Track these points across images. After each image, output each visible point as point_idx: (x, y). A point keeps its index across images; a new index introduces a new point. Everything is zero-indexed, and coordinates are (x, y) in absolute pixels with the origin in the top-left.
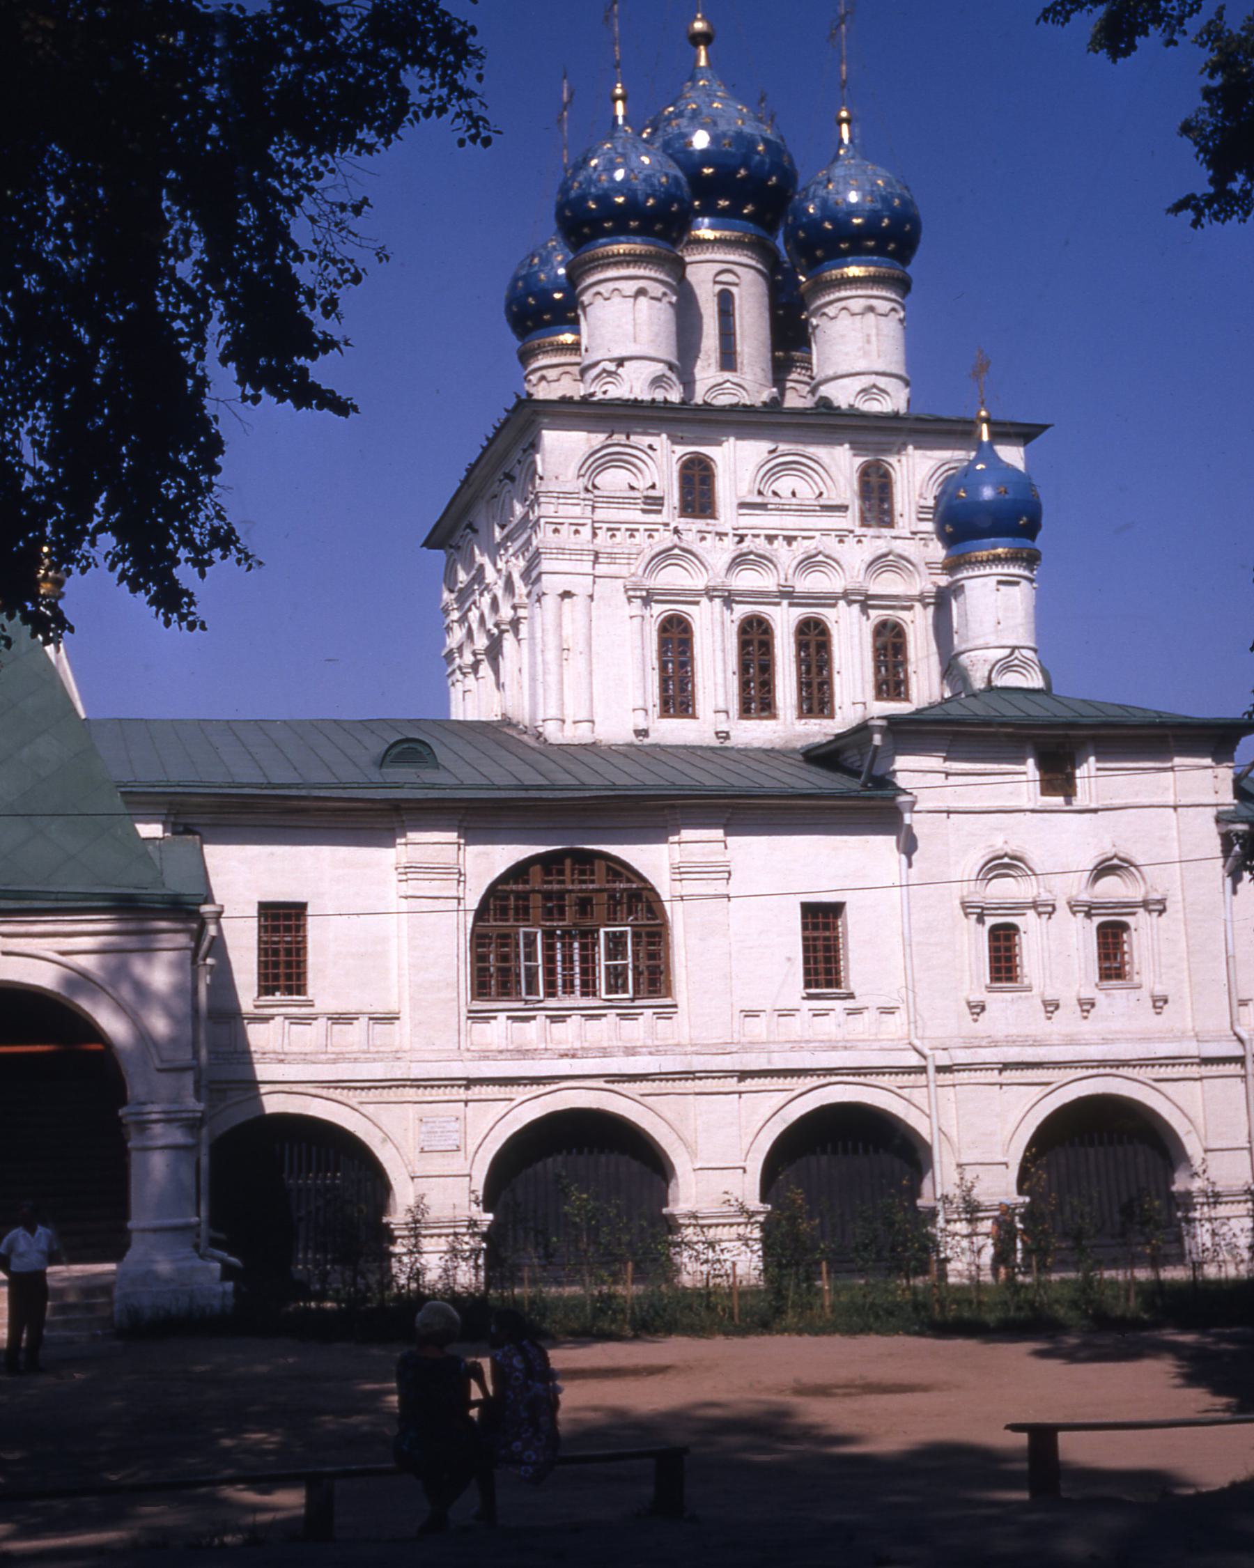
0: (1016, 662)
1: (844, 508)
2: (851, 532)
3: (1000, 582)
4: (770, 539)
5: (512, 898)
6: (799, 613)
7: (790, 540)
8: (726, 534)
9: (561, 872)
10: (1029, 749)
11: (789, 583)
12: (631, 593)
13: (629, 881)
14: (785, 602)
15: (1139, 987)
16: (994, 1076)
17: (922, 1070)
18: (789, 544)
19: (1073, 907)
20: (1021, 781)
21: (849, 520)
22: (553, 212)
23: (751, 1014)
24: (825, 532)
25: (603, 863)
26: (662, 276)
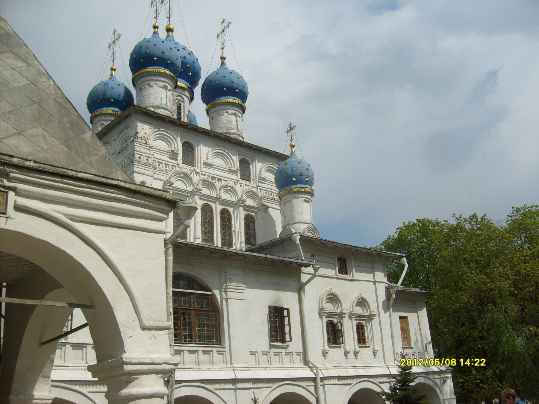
2: (239, 181)
3: (305, 201)
4: (213, 178)
8: (199, 173)
14: (218, 203)
15: (369, 347)
16: (336, 381)
17: (314, 380)
21: (237, 177)
23: (252, 353)
26: (171, 84)
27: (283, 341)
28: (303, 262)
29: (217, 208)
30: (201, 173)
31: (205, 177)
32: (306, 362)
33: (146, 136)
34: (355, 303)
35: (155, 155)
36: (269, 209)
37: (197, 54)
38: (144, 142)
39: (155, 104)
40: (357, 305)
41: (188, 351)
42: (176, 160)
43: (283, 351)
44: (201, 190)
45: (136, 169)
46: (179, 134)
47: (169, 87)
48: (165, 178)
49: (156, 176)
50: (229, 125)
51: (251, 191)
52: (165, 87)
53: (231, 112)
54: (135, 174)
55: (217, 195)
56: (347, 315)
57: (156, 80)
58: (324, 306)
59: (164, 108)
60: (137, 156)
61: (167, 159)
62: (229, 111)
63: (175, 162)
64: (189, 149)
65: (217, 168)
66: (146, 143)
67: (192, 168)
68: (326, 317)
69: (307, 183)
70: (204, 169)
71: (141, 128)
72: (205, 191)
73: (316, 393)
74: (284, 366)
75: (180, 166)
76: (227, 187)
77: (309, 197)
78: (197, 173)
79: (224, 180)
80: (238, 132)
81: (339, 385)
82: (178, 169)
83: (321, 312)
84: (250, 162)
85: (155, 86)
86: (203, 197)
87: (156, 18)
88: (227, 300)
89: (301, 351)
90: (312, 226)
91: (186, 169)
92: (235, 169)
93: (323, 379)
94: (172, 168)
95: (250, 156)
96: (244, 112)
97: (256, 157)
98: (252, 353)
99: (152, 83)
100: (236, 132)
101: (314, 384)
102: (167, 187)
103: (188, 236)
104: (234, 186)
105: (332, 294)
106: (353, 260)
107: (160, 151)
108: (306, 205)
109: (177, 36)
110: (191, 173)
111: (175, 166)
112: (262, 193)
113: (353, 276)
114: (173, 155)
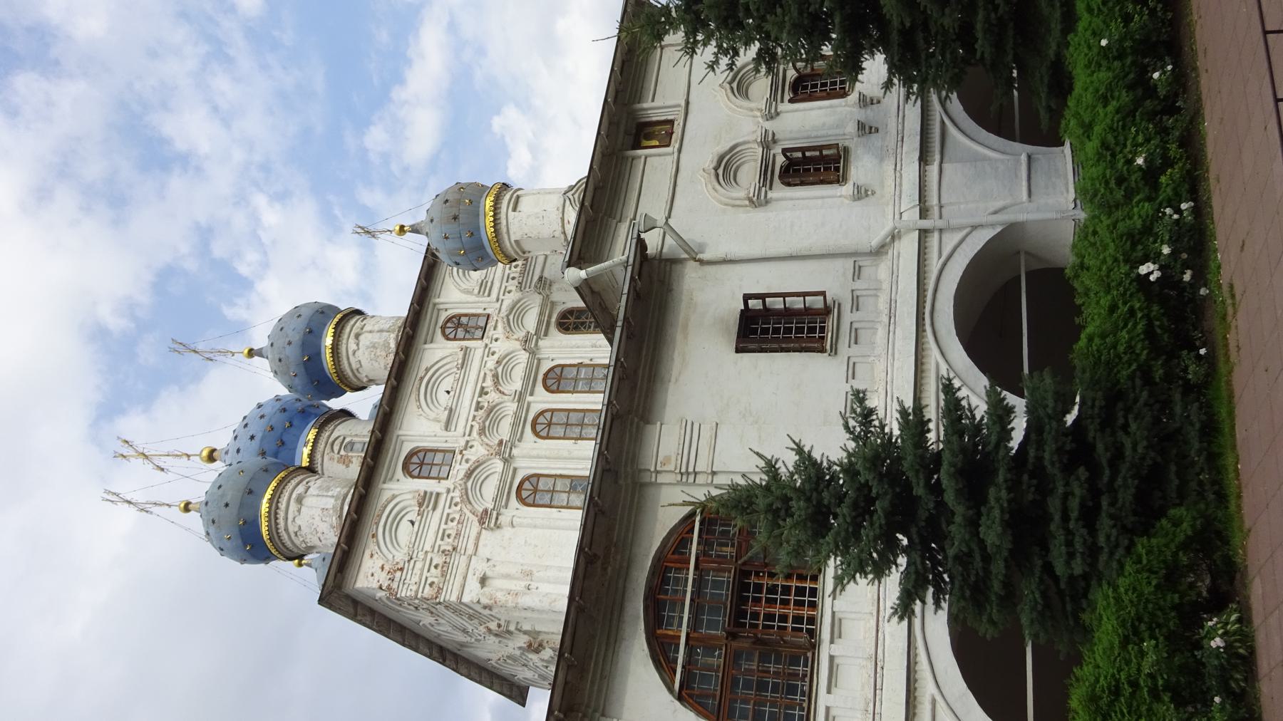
3: (514, 210)
6: (539, 388)
7: (483, 392)
8: (468, 442)
12: (492, 525)
14: (529, 398)
16: (933, 170)
17: (924, 234)
18: (486, 393)
19: (772, 115)
20: (654, 167)
22: (262, 565)
24: (483, 363)
27: (827, 311)
28: (631, 260)
29: (542, 400)
30: (467, 438)
31: (476, 427)
32: (879, 251)
33: (387, 568)
34: (741, 102)
35: (428, 547)
36: (546, 275)
37: (248, 408)
38: (399, 573)
40: (746, 96)
42: (438, 494)
43: (847, 317)
44: (501, 442)
45: (454, 598)
46: (385, 486)
47: (301, 489)
48: (475, 527)
49: (470, 550)
51: (508, 316)
52: (300, 500)
53: (352, 346)
54: (466, 599)
56: (769, 125)
57: (286, 519)
58: (742, 194)
60: (428, 592)
64: (419, 463)
66: (402, 569)
68: (771, 188)
69: (475, 204)
70: (460, 429)
71: (370, 578)
72: (505, 430)
73: (960, 228)
76: (496, 376)
77: (508, 196)
78: (467, 446)
81: (941, 162)
83: (758, 202)
84: (451, 312)
85: (298, 522)
86: (517, 436)
87: (169, 506)
90: (570, 194)
91: (459, 469)
92: (461, 354)
93: (924, 213)
94: (456, 505)
96: (358, 312)
97: (437, 300)
99: (292, 529)
101: (936, 235)
102: (492, 525)
104: (496, 357)
105: (716, 169)
106: (645, 105)
108: (524, 204)
109: (222, 441)
110: (467, 461)
112: (513, 288)
113: (679, 106)
114: (426, 501)
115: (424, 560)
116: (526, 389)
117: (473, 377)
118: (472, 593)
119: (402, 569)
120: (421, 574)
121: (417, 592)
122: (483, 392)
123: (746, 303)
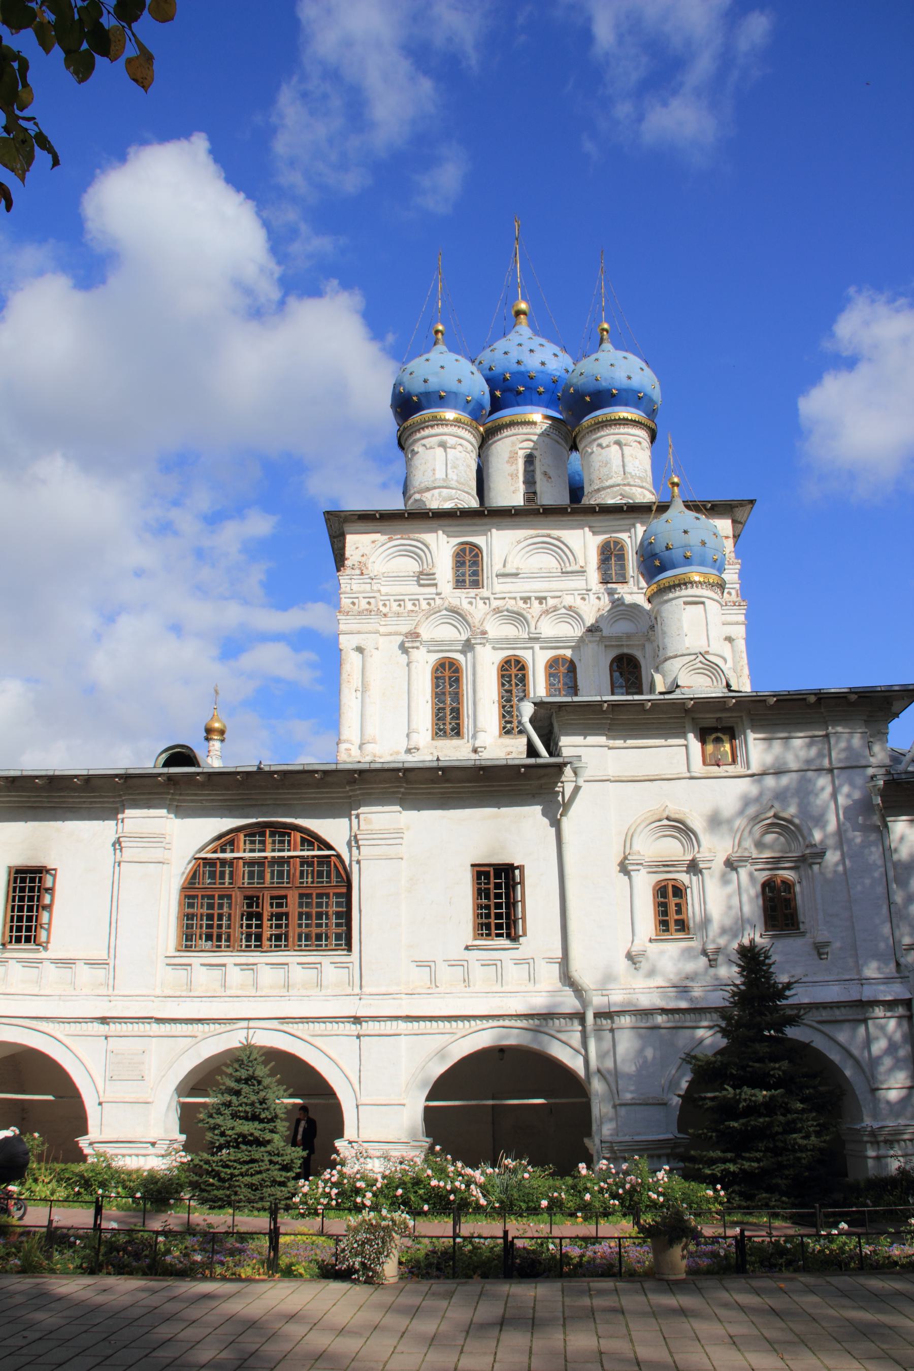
0: (701, 665)
1: (582, 572)
3: (686, 603)
4: (526, 600)
5: (218, 865)
7: (541, 600)
8: (488, 599)
9: (263, 842)
10: (688, 725)
11: (537, 631)
13: (320, 849)
23: (420, 964)
25: (299, 835)
30: (492, 597)
32: (567, 979)
35: (384, 590)
38: (358, 572)
39: (422, 485)
41: (267, 964)
42: (436, 585)
45: (342, 627)
48: (405, 629)
50: (604, 470)
53: (604, 442)
55: (529, 633)
57: (423, 438)
59: (435, 488)
61: (414, 588)
62: (600, 441)
63: (432, 590)
65: (532, 577)
66: (362, 574)
67: (473, 592)
71: (354, 547)
74: (503, 989)
75: (442, 596)
76: (555, 609)
78: (485, 599)
79: (552, 597)
80: (625, 478)
82: (438, 602)
86: (498, 645)
88: (358, 862)
89: (559, 954)
90: (701, 658)
92: (577, 568)
95: (628, 527)
98: (420, 964)
100: (619, 480)
103: (465, 730)
107: (397, 578)
111: (434, 599)
115: (372, 591)
116: (546, 642)
117: (555, 585)
118: (347, 643)
119: (362, 574)
120: (360, 592)
121: (345, 593)
122: (541, 600)
123: (517, 867)
